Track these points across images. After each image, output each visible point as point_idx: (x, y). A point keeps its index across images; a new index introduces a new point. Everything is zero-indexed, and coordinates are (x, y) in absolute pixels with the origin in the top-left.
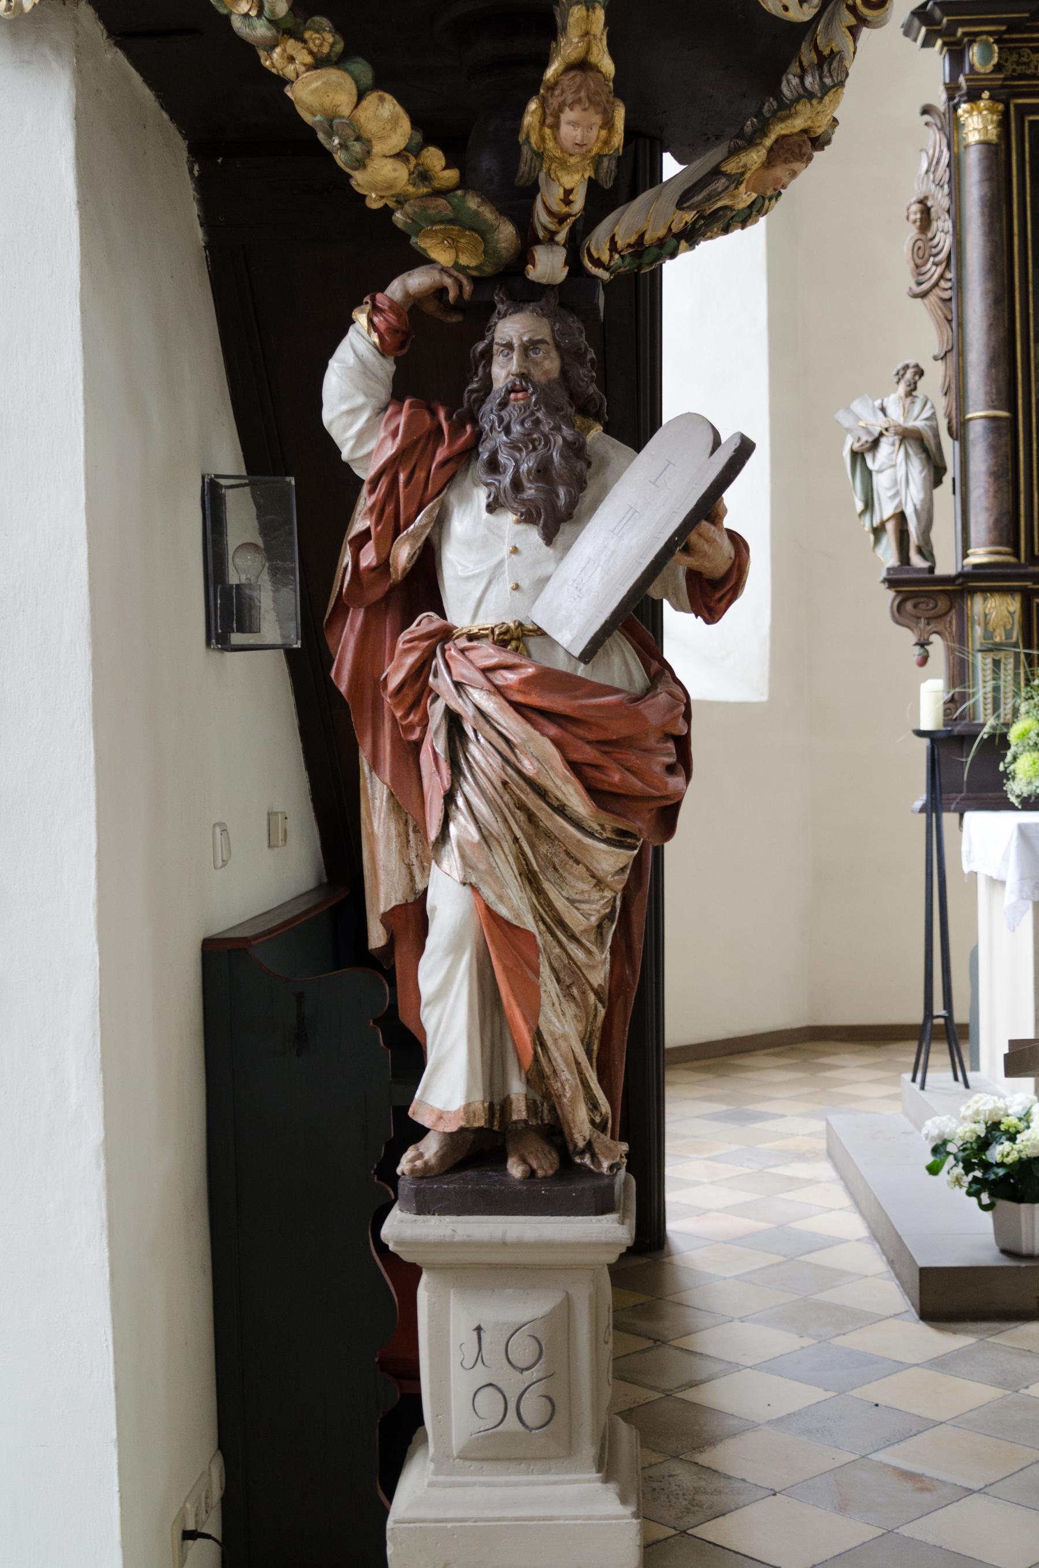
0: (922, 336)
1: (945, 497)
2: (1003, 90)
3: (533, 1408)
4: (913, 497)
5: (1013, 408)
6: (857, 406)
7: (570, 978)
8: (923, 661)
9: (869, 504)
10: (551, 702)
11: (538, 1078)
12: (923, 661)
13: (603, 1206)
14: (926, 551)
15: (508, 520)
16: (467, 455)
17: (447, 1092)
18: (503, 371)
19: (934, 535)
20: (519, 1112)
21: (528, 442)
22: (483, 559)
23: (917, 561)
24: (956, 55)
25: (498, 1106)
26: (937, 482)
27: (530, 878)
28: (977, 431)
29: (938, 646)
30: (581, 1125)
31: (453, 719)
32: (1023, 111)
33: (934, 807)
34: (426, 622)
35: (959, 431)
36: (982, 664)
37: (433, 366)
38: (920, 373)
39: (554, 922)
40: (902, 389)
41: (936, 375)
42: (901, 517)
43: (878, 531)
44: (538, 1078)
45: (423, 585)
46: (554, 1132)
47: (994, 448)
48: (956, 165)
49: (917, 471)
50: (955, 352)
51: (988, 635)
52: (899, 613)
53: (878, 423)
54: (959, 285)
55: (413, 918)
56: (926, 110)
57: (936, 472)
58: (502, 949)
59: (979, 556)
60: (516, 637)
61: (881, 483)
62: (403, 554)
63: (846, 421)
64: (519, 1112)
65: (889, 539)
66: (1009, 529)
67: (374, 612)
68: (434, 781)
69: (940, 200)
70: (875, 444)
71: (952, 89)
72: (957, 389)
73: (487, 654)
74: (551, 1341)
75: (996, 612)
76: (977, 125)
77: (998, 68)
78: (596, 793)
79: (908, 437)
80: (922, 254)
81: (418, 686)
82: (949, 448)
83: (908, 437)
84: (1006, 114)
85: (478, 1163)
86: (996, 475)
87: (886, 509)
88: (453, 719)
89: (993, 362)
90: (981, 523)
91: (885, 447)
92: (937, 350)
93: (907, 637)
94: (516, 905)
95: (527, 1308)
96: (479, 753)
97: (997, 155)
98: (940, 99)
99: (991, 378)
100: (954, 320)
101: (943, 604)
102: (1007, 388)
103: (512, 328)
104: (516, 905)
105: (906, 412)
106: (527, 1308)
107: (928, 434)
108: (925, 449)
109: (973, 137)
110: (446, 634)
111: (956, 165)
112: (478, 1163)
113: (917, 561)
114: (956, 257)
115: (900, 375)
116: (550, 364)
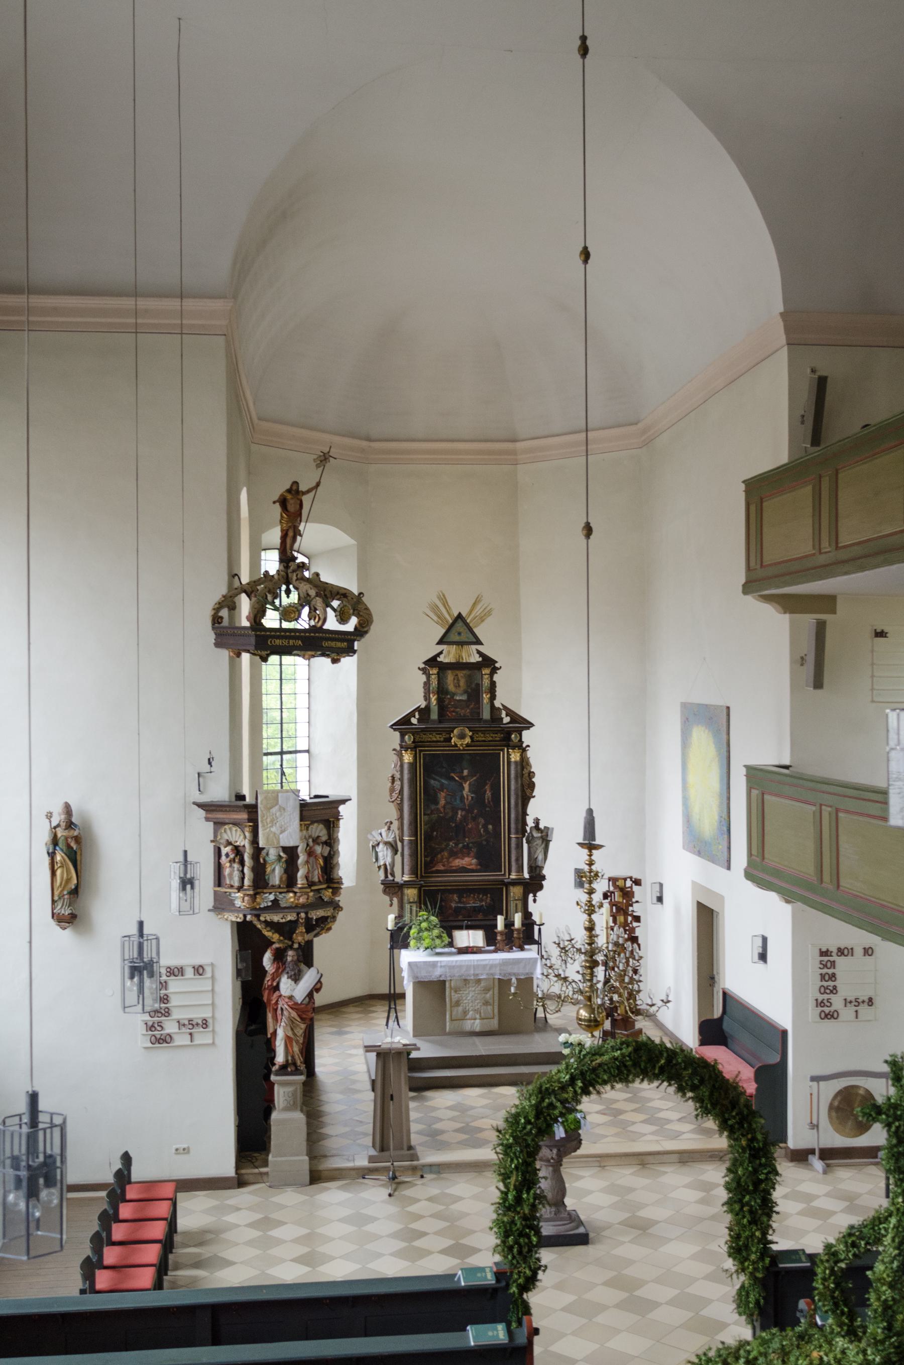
0: (392, 813)
1: (398, 857)
2: (415, 747)
3: (292, 1103)
4: (389, 860)
5: (416, 835)
6: (374, 833)
7: (297, 1042)
8: (391, 905)
9: (377, 859)
10: (295, 1007)
11: (293, 1057)
12: (391, 905)
13: (301, 1074)
14: (393, 875)
15: (290, 980)
16: (284, 969)
17: (280, 1058)
18: (289, 959)
19: (395, 869)
20: (290, 1061)
21: (292, 970)
22: (286, 985)
23: (390, 878)
24: (402, 736)
25: (287, 1061)
26: (396, 854)
27: (292, 1029)
28: (406, 843)
29: (395, 900)
30: (299, 1063)
31: (282, 1009)
32: (421, 751)
33: (392, 948)
34: (277, 993)
35: (402, 841)
36: (407, 907)
37: (279, 956)
38: (391, 823)
39: (295, 1034)
40: (386, 828)
41: (396, 824)
42: (385, 865)
43: (379, 867)
44: (293, 1057)
45: (277, 988)
46: (294, 1064)
47: (410, 848)
48: (402, 766)
49: (390, 853)
50: (401, 818)
51: (408, 900)
52: (385, 892)
53: (379, 838)
54: (402, 800)
55: (275, 1033)
56: (394, 750)
57: (395, 851)
58: (288, 1040)
59: (406, 878)
60: (291, 998)
61: (380, 855)
62: (275, 984)
63: (370, 837)
64: (290, 1061)
65: (382, 870)
66: (414, 871)
67: (270, 990)
68: (279, 1017)
69: (398, 775)
70: (378, 844)
71: (401, 747)
72: (401, 828)
73: (287, 1000)
74: (294, 1094)
75: (411, 893)
76: (408, 758)
77: (414, 742)
78: (301, 1018)
79: (386, 843)
80: (392, 790)
81: (277, 1003)
82: (399, 844)
83: (386, 843)
84: (416, 754)
85: (283, 1070)
86: (410, 856)
87: (381, 863)
88: (282, 1009)
89: (410, 824)
90: (407, 868)
91: (381, 846)
92: (396, 817)
93: (387, 898)
94: (290, 1034)
95: (290, 1089)
96: (285, 1013)
97: (413, 766)
98: (398, 748)
99: (410, 829)
100: (401, 810)
101: (397, 889)
102: (414, 832)
103: (290, 953)
104: (290, 1034)
105: (387, 835)
106: (290, 1089)
107: (393, 843)
108: (392, 846)
109: (406, 761)
110: (281, 996)
111: (402, 766)
112: (283, 1070)
113: (390, 878)
114: (401, 792)
115: (386, 824)
116: (296, 958)
